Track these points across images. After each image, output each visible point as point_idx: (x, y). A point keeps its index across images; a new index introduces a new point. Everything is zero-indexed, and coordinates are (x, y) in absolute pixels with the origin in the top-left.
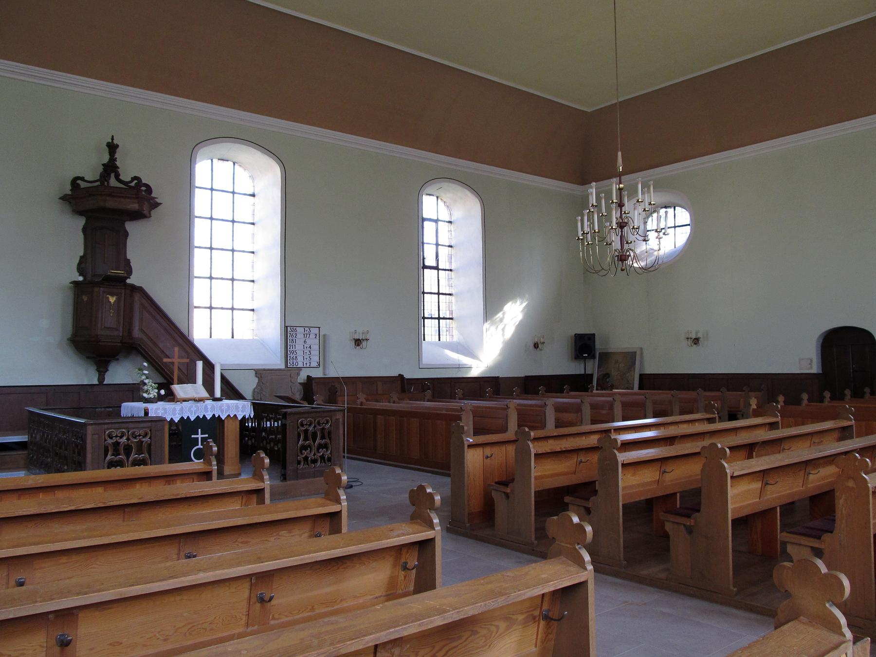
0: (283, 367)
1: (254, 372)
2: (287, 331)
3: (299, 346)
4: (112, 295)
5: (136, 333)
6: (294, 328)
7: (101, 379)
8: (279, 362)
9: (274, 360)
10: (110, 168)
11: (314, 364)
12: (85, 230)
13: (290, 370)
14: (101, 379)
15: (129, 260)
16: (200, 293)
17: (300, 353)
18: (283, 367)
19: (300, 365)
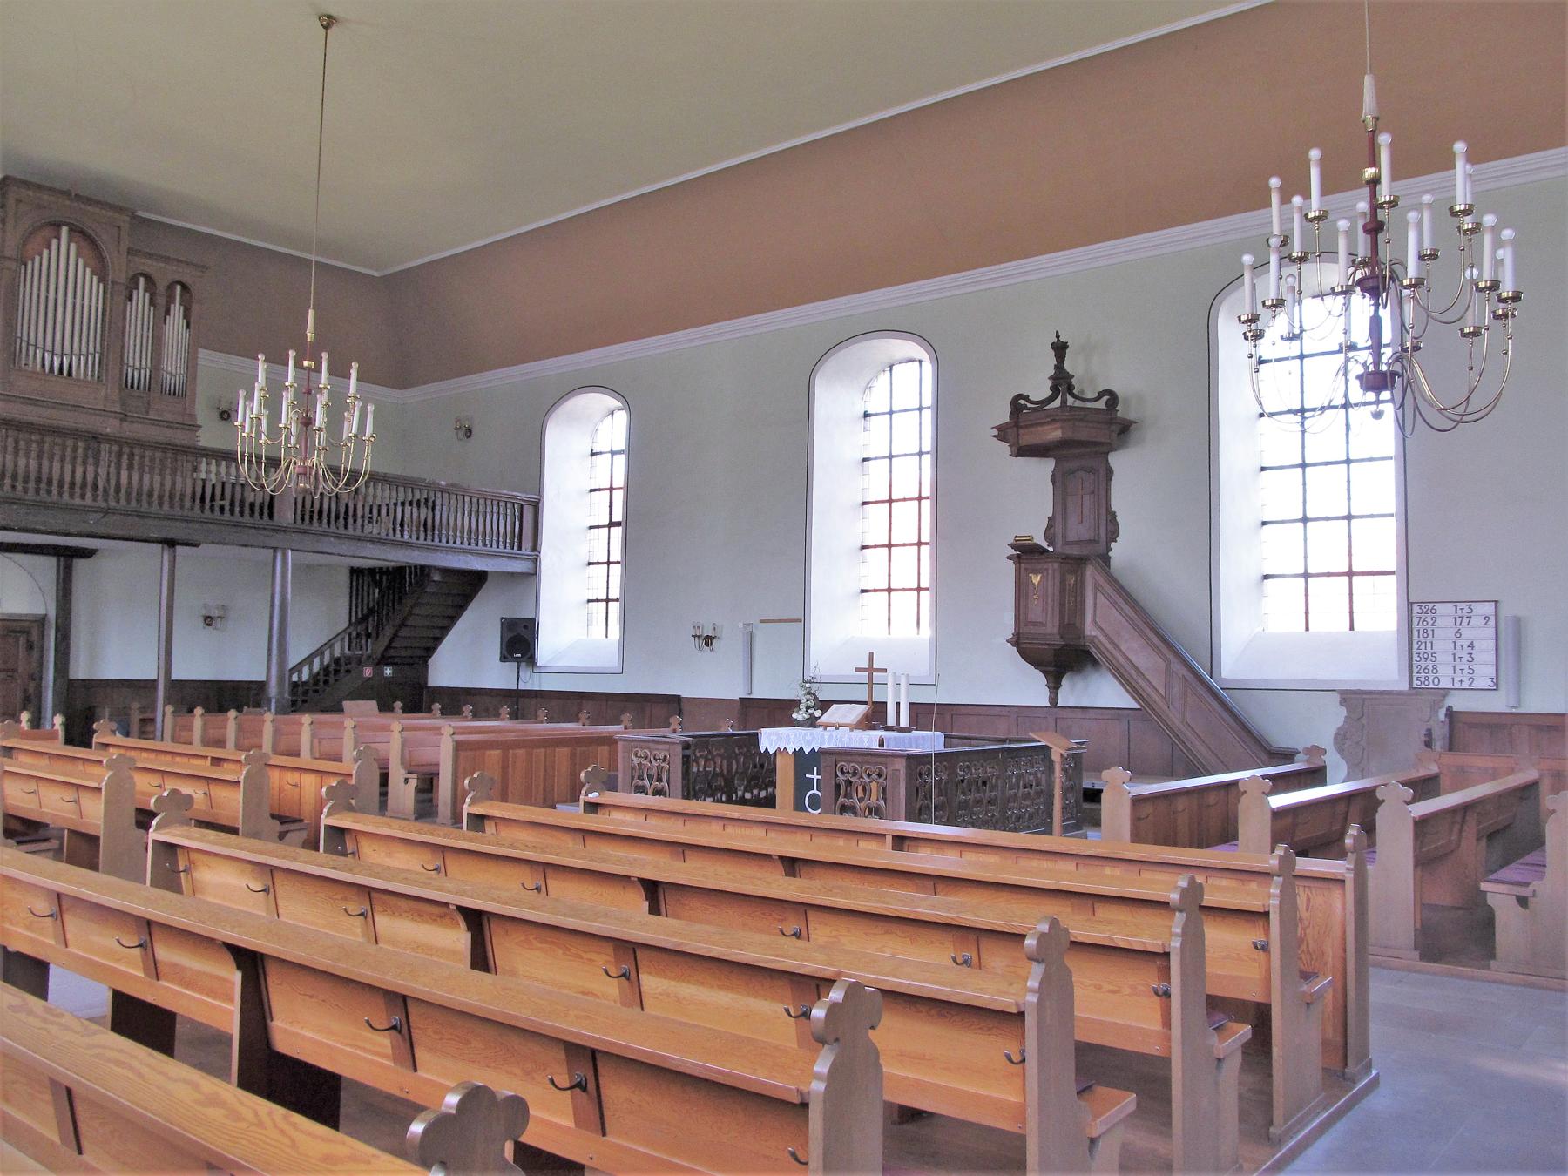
0: (1405, 687)
1: (1336, 697)
2: (1415, 613)
3: (1442, 643)
4: (1036, 572)
5: (1090, 630)
6: (1429, 606)
7: (1054, 699)
8: (1396, 676)
9: (1383, 670)
10: (1062, 381)
11: (1483, 682)
12: (1053, 478)
13: (1422, 695)
14: (1054, 699)
15: (1114, 515)
16: (1243, 552)
17: (1444, 659)
18: (1405, 687)
19: (1445, 683)
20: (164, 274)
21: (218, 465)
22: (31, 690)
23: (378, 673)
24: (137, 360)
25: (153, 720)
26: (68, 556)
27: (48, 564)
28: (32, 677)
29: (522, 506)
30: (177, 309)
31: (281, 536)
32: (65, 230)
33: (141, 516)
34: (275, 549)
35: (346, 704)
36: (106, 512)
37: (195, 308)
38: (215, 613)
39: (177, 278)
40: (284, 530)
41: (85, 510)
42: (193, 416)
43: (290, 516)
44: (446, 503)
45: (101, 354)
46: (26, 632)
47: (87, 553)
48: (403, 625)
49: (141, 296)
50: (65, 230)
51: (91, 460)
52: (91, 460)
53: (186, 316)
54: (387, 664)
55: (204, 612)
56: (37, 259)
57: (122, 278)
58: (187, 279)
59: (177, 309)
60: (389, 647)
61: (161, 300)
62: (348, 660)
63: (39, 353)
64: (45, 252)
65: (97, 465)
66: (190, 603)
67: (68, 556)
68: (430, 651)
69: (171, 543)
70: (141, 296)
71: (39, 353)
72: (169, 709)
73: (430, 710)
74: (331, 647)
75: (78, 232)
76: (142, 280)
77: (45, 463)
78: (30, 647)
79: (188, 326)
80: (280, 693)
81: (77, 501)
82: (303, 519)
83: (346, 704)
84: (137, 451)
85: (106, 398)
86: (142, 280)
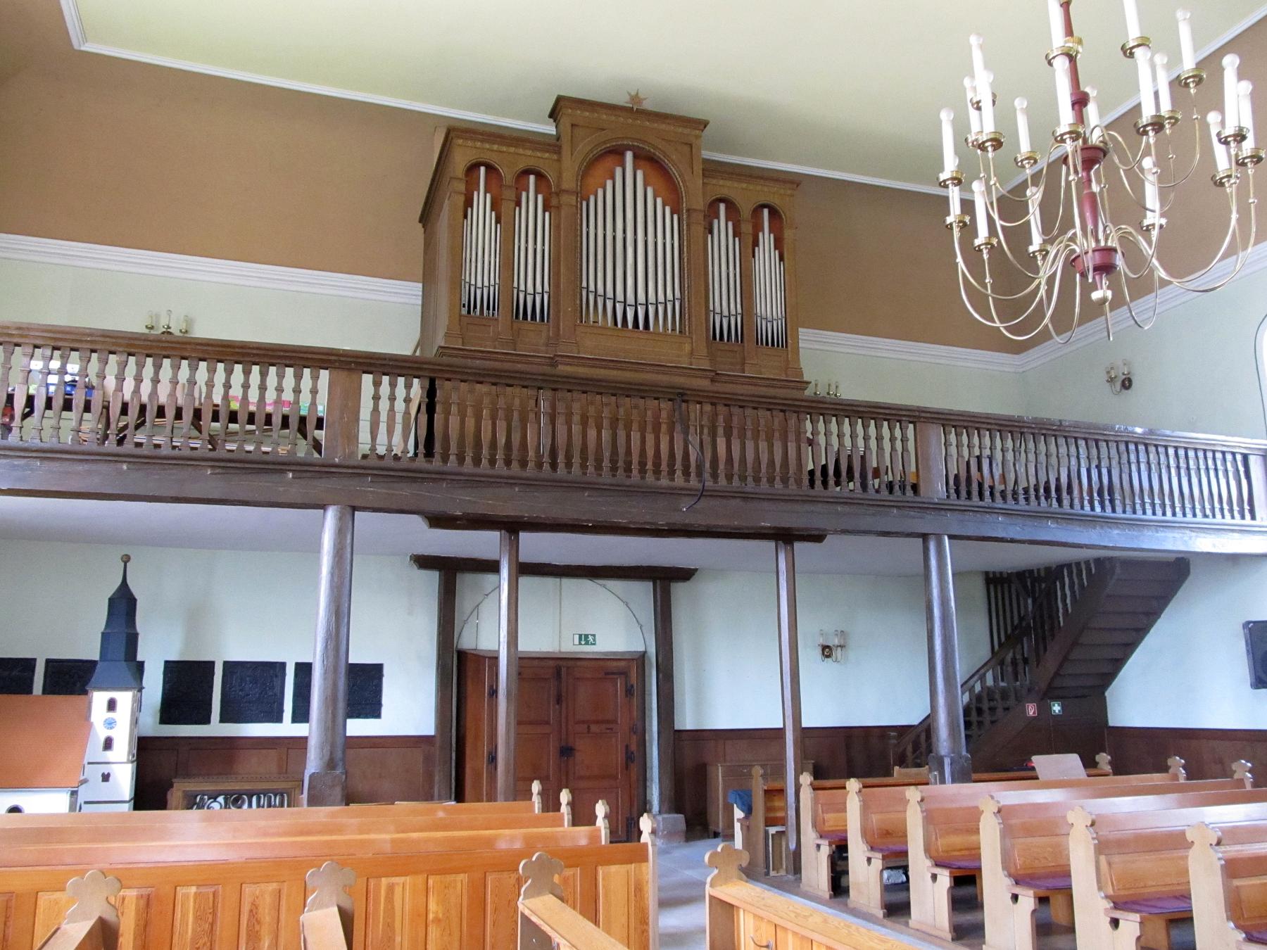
20: (746, 196)
21: (839, 424)
22: (633, 748)
23: (1044, 709)
24: (723, 303)
25: (781, 792)
26: (665, 580)
27: (642, 592)
28: (633, 730)
29: (1245, 458)
30: (766, 239)
31: (930, 517)
32: (629, 156)
33: (746, 497)
34: (925, 537)
35: (1038, 761)
36: (702, 494)
37: (788, 234)
38: (834, 641)
39: (763, 200)
40: (938, 508)
41: (673, 493)
42: (800, 372)
43: (941, 487)
44: (1143, 458)
45: (682, 300)
46: (624, 673)
47: (685, 575)
48: (1075, 644)
49: (722, 225)
50: (629, 156)
51: (678, 427)
52: (678, 427)
53: (779, 244)
54: (1056, 698)
55: (821, 641)
56: (600, 192)
57: (700, 203)
58: (775, 201)
59: (766, 239)
60: (1057, 674)
61: (747, 228)
62: (1004, 694)
63: (609, 304)
64: (609, 183)
65: (686, 432)
66: (811, 631)
67: (665, 580)
68: (1109, 677)
69: (785, 537)
70: (722, 225)
71: (609, 304)
72: (806, 779)
73: (1164, 769)
74: (983, 678)
75: (646, 159)
76: (722, 207)
77: (621, 434)
78: (629, 692)
79: (781, 259)
80: (954, 749)
81: (664, 482)
82: (957, 492)
83: (1038, 761)
84: (735, 410)
85: (692, 353)
86: (722, 207)
